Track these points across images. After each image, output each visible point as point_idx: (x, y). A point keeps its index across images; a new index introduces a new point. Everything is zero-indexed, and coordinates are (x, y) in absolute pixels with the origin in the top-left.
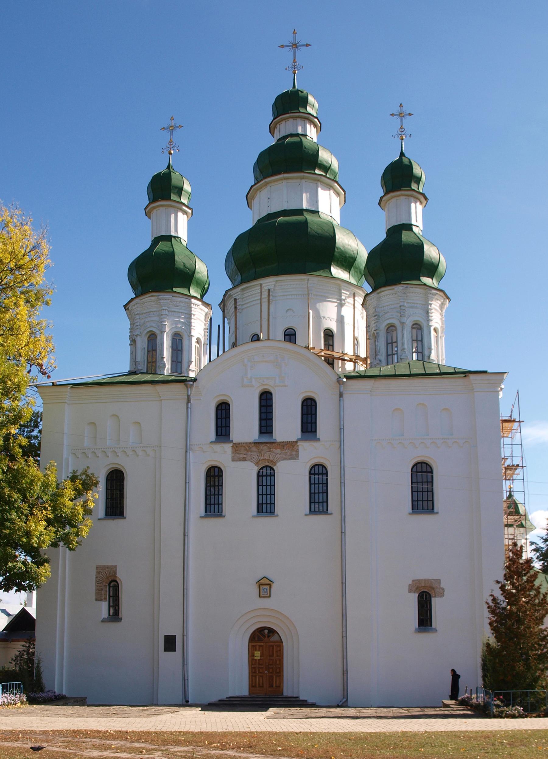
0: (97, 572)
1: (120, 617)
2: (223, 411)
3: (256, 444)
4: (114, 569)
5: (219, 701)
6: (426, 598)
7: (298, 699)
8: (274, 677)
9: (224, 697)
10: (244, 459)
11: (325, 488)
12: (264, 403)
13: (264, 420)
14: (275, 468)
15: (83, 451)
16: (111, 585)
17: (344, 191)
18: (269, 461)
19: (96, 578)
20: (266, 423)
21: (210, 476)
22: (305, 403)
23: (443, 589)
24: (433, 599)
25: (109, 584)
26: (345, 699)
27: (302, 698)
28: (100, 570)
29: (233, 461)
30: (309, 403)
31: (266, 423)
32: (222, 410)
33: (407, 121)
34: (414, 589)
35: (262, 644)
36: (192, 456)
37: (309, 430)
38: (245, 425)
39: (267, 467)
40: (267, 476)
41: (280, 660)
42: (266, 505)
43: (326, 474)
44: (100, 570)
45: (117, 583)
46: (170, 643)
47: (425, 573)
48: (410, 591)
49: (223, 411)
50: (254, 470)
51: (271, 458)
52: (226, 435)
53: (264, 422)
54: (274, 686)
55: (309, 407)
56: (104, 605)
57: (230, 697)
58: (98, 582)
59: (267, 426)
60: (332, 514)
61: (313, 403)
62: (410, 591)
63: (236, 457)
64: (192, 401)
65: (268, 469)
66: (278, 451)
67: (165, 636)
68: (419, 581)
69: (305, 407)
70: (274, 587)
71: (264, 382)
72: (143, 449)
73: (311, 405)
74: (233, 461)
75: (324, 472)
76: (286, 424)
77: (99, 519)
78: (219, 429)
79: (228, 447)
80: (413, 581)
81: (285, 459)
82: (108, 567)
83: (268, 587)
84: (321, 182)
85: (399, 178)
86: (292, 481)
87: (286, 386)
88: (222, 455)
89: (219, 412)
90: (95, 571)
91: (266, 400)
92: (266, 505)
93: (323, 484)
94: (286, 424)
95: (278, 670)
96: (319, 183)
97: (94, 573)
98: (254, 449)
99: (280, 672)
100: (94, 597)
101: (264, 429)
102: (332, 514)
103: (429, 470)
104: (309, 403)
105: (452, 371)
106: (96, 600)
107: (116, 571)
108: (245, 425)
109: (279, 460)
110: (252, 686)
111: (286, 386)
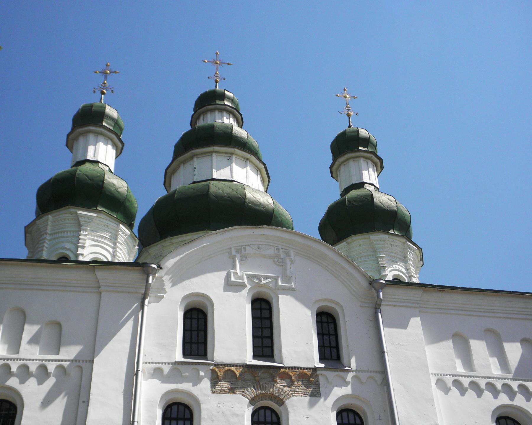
17: (269, 178)
29: (213, 392)
32: (191, 318)
38: (232, 340)
39: (266, 408)
55: (327, 324)
59: (263, 347)
65: (268, 413)
71: (260, 281)
84: (250, 161)
89: (188, 321)
96: (248, 162)
108: (232, 340)
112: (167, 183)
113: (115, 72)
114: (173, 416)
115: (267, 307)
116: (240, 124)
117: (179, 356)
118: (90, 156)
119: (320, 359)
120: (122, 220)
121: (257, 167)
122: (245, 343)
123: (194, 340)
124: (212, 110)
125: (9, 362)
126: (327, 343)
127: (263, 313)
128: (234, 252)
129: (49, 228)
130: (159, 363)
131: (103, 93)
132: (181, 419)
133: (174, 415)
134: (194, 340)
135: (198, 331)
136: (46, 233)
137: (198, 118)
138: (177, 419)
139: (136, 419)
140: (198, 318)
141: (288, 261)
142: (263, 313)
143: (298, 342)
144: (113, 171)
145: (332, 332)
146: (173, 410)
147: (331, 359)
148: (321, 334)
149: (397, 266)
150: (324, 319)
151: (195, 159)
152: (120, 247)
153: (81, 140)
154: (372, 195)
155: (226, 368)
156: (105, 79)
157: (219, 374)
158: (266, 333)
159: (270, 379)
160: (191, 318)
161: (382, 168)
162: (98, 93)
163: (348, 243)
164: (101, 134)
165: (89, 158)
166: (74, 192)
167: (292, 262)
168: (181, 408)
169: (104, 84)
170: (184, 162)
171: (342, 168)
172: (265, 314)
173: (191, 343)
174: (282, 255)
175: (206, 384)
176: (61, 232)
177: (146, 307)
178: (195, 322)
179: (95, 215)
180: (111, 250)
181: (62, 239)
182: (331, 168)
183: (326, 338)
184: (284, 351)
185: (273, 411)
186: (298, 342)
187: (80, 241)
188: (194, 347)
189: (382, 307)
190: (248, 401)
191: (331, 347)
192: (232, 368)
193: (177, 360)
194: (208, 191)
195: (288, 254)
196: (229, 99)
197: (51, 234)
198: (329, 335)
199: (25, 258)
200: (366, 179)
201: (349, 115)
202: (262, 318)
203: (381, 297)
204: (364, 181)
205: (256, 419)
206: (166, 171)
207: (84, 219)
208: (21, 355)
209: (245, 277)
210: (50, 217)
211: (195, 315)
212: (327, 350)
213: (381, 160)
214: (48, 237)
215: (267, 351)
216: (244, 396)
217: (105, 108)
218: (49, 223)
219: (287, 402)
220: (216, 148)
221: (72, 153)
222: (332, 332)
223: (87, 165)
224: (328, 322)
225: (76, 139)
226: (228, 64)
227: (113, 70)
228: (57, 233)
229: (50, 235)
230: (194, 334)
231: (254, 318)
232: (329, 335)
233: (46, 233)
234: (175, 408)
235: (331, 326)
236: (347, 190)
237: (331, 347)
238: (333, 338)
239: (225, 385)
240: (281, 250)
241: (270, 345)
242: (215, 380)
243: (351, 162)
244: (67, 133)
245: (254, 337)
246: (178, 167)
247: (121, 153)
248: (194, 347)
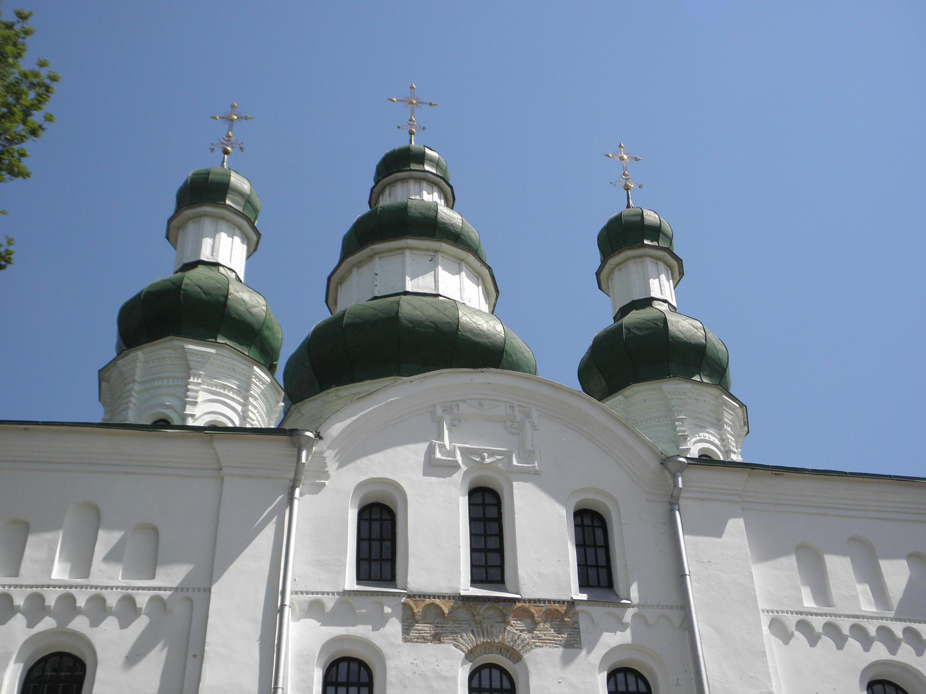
12: (479, 512)
17: (497, 291)
21: (337, 684)
29: (406, 640)
32: (370, 520)
38: (438, 555)
39: (491, 666)
55: (592, 530)
65: (496, 674)
71: (483, 458)
72: (157, 592)
84: (466, 263)
89: (365, 524)
96: (464, 264)
108: (438, 555)
109: (528, 646)
112: (330, 298)
113: (246, 118)
114: (340, 680)
115: (495, 502)
116: (451, 202)
117: (350, 582)
118: (205, 255)
119: (580, 586)
120: (258, 359)
121: (477, 272)
122: (458, 561)
123: (375, 555)
124: (404, 180)
125: (73, 591)
126: (592, 561)
127: (488, 512)
128: (439, 412)
129: (138, 372)
130: (317, 593)
131: (226, 152)
132: (353, 684)
133: (342, 678)
134: (375, 555)
135: (381, 540)
136: (134, 381)
137: (382, 192)
138: (347, 685)
139: (280, 685)
140: (381, 520)
141: (528, 426)
142: (488, 512)
143: (544, 558)
144: (242, 278)
145: (600, 542)
146: (340, 670)
147: (599, 586)
148: (581, 545)
150: (587, 521)
151: (377, 260)
152: (255, 403)
153: (191, 227)
154: (665, 319)
155: (428, 601)
156: (230, 129)
157: (415, 611)
158: (493, 543)
159: (499, 619)
160: (370, 520)
161: (682, 274)
162: (219, 151)
163: (626, 397)
164: (223, 218)
166: (177, 313)
167: (535, 428)
168: (354, 666)
169: (229, 136)
170: (359, 265)
171: (617, 275)
172: (491, 512)
173: (370, 560)
174: (519, 417)
175: (394, 627)
176: (159, 379)
177: (296, 502)
178: (376, 526)
179: (213, 351)
180: (239, 408)
182: (598, 274)
183: (591, 551)
184: (522, 573)
185: (503, 671)
186: (544, 558)
187: (189, 393)
188: (375, 566)
189: (681, 502)
190: (463, 654)
191: (597, 567)
192: (437, 601)
193: (347, 588)
194: (398, 312)
195: (528, 415)
196: (433, 162)
198: (595, 546)
199: (100, 421)
200: (655, 293)
201: (627, 188)
203: (680, 486)
204: (653, 295)
205: (475, 684)
206: (329, 279)
207: (195, 358)
208: (93, 580)
209: (458, 453)
210: (140, 355)
212: (592, 572)
213: (679, 260)
214: (137, 387)
216: (456, 646)
217: (230, 176)
218: (139, 364)
219: (526, 656)
220: (411, 242)
221: (175, 247)
222: (600, 542)
223: (201, 269)
224: (593, 526)
225: (182, 227)
226: (430, 104)
227: (243, 115)
228: (151, 380)
231: (472, 520)
232: (595, 546)
233: (134, 381)
234: (343, 667)
235: (599, 533)
236: (624, 311)
237: (597, 567)
238: (601, 552)
239: (425, 628)
240: (516, 408)
241: (499, 564)
242: (409, 621)
243: (632, 266)
244: (168, 217)
245: (473, 550)
246: (350, 271)
247: (255, 249)
248: (375, 566)
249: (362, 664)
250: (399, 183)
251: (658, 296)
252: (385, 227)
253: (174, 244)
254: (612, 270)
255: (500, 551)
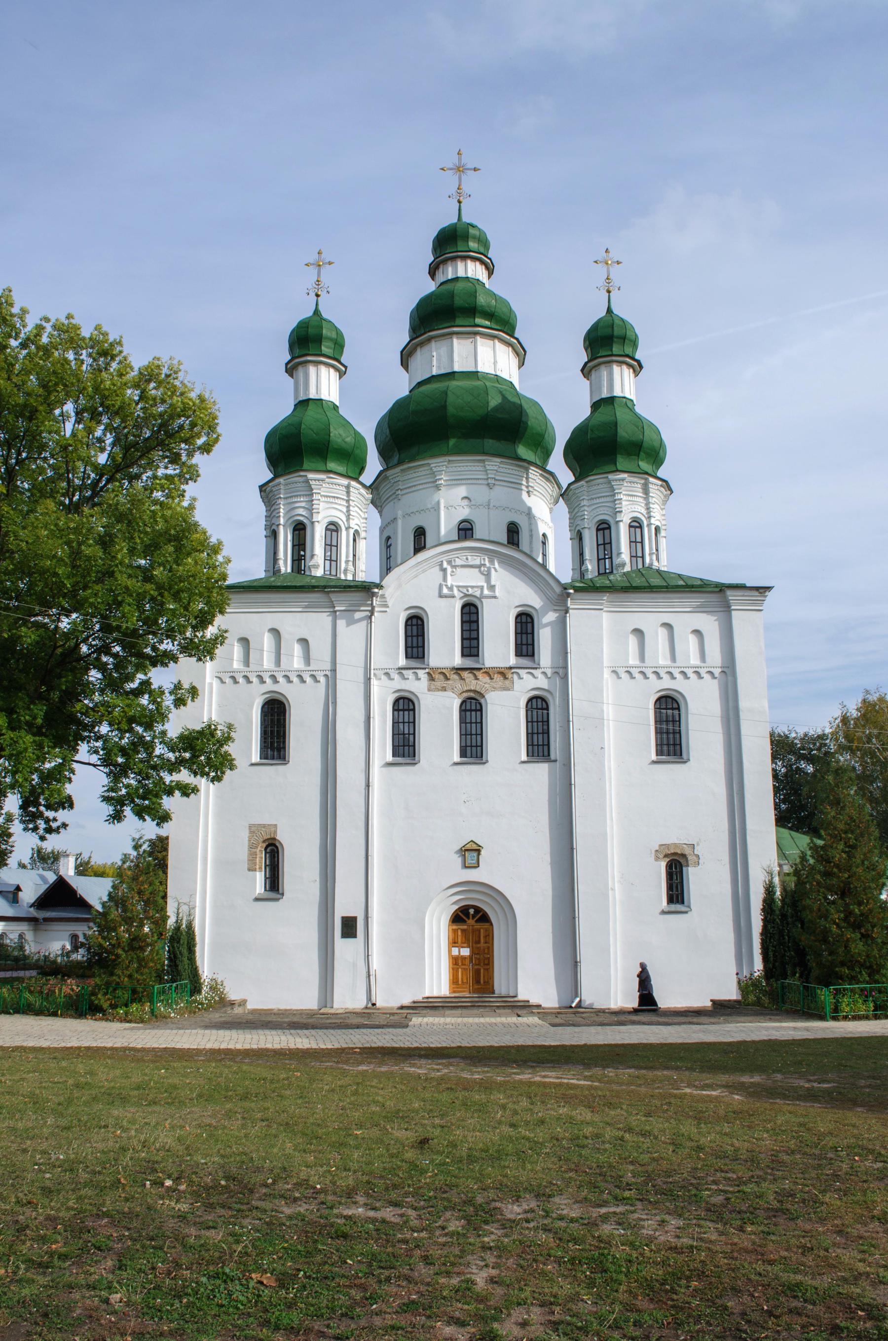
0: (251, 832)
1: (280, 891)
2: (416, 627)
3: (458, 670)
4: (273, 829)
5: (414, 1002)
6: (676, 868)
7: (516, 999)
8: (482, 971)
9: (419, 998)
10: (444, 689)
11: (545, 727)
13: (466, 639)
14: (482, 701)
15: (232, 674)
16: (268, 850)
18: (475, 691)
19: (249, 841)
20: (471, 643)
21: (398, 710)
22: (519, 620)
23: (698, 856)
24: (684, 869)
25: (266, 849)
26: (578, 999)
27: (521, 997)
28: (253, 829)
29: (429, 690)
30: (524, 620)
31: (471, 643)
32: (412, 625)
33: (615, 271)
34: (661, 856)
35: (465, 927)
36: (374, 682)
37: (524, 652)
40: (471, 710)
41: (488, 948)
42: (473, 748)
43: (547, 709)
44: (253, 829)
45: (277, 847)
46: (349, 927)
47: (675, 837)
48: (657, 859)
49: (416, 627)
50: (456, 703)
51: (478, 689)
52: (418, 658)
53: (467, 643)
54: (482, 982)
55: (525, 624)
56: (259, 879)
57: (428, 998)
58: (252, 847)
60: (555, 761)
61: (529, 620)
62: (657, 859)
63: (433, 687)
64: (376, 614)
66: (487, 679)
67: (343, 918)
68: (667, 846)
69: (519, 625)
70: (482, 852)
73: (527, 623)
74: (429, 690)
75: (544, 706)
76: (498, 646)
77: (252, 765)
78: (409, 650)
79: (422, 673)
80: (661, 845)
81: (495, 689)
82: (264, 826)
83: (475, 854)
85: (607, 342)
86: (506, 718)
87: (495, 597)
88: (416, 683)
89: (409, 628)
90: (247, 831)
91: (471, 614)
92: (473, 748)
93: (543, 722)
94: (498, 646)
95: (486, 962)
97: (245, 834)
98: (456, 677)
99: (488, 964)
100: (246, 866)
101: (466, 651)
102: (555, 761)
103: (675, 706)
104: (524, 620)
105: (699, 583)
106: (249, 870)
107: (275, 832)
110: (454, 981)
111: (495, 597)
117: (402, 661)
118: (313, 395)
123: (415, 645)
124: (454, 259)
125: (274, 673)
128: (445, 565)
129: (282, 491)
131: (318, 296)
133: (401, 707)
134: (415, 645)
135: (418, 636)
138: (404, 710)
140: (417, 625)
141: (493, 570)
149: (636, 507)
151: (433, 344)
153: (301, 370)
154: (616, 423)
160: (412, 625)
161: (641, 367)
162: (313, 295)
165: (312, 396)
170: (421, 344)
173: (412, 647)
181: (297, 505)
183: (524, 636)
184: (486, 655)
187: (314, 507)
189: (571, 611)
192: (444, 671)
194: (446, 401)
197: (284, 498)
198: (527, 633)
202: (470, 622)
204: (615, 394)
206: (402, 352)
209: (455, 589)
210: (281, 480)
211: (414, 621)
213: (638, 362)
215: (474, 651)
217: (322, 328)
226: (475, 169)
227: (327, 261)
228: (291, 497)
229: (284, 498)
230: (415, 639)
231: (463, 622)
232: (527, 633)
234: (401, 701)
238: (530, 636)
242: (431, 678)
243: (603, 367)
249: (410, 700)
250: (449, 263)
251: (620, 394)
252: (440, 314)
253: (291, 376)
254: (590, 371)
255: (477, 639)
